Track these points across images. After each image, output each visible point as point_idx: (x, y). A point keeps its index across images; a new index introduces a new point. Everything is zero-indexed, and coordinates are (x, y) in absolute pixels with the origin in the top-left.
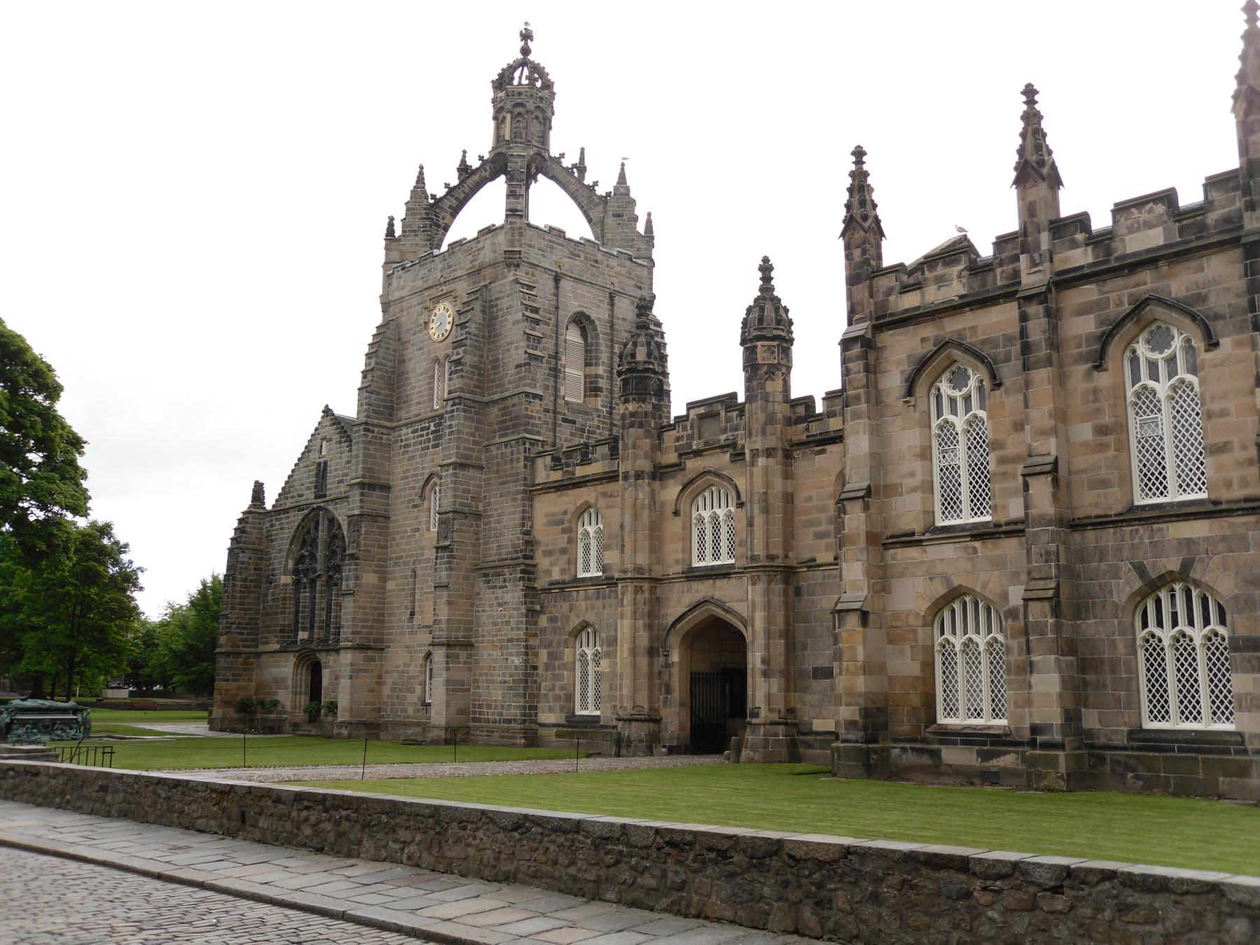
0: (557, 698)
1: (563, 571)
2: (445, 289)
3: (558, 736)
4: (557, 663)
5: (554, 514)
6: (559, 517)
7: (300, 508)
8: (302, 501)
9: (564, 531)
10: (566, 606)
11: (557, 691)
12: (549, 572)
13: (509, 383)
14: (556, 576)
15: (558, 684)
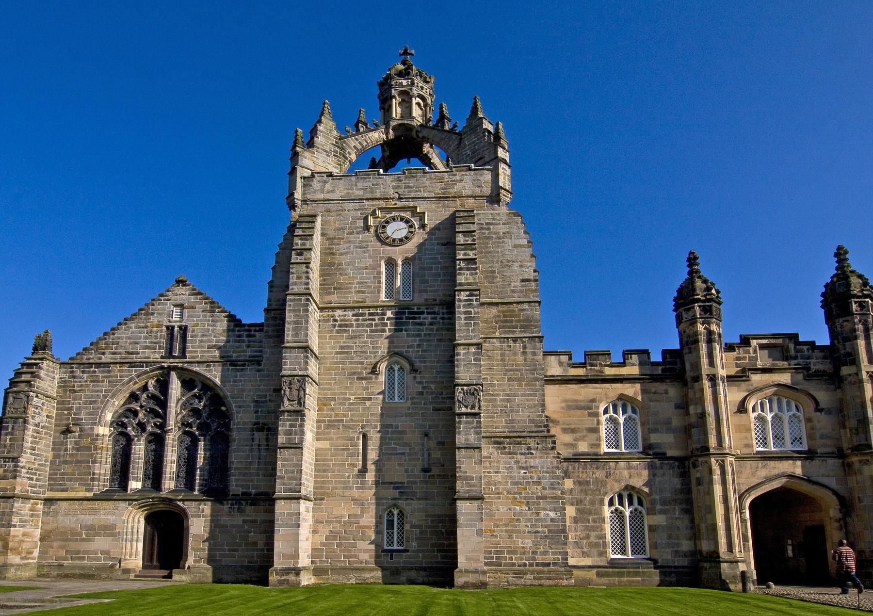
0: (596, 545)
1: (592, 446)
2: (411, 204)
3: (598, 574)
4: (590, 518)
5: (576, 401)
6: (583, 404)
7: (132, 365)
8: (134, 358)
9: (590, 415)
10: (600, 474)
11: (592, 539)
12: (573, 446)
13: (513, 291)
14: (583, 447)
15: (593, 534)
